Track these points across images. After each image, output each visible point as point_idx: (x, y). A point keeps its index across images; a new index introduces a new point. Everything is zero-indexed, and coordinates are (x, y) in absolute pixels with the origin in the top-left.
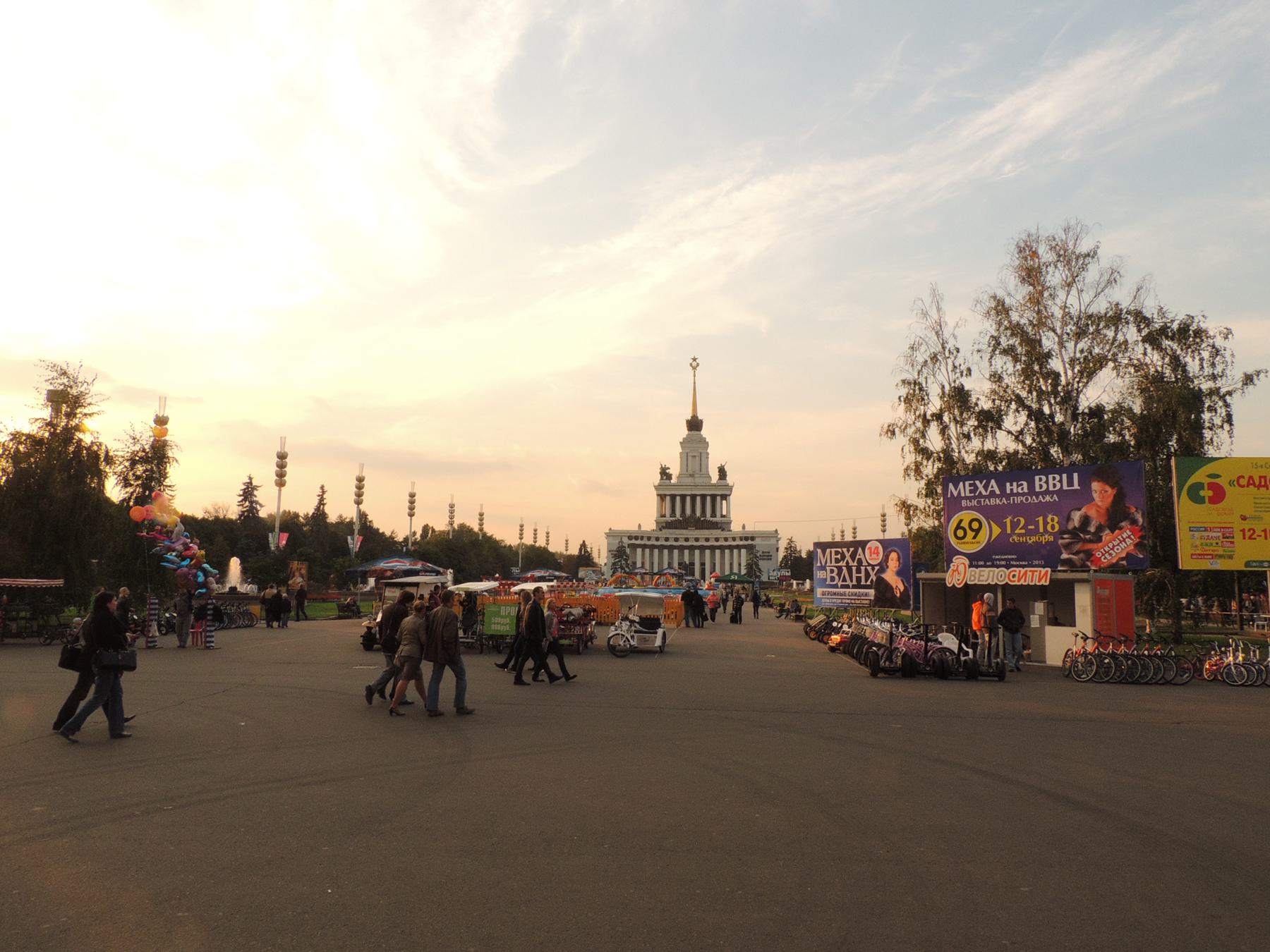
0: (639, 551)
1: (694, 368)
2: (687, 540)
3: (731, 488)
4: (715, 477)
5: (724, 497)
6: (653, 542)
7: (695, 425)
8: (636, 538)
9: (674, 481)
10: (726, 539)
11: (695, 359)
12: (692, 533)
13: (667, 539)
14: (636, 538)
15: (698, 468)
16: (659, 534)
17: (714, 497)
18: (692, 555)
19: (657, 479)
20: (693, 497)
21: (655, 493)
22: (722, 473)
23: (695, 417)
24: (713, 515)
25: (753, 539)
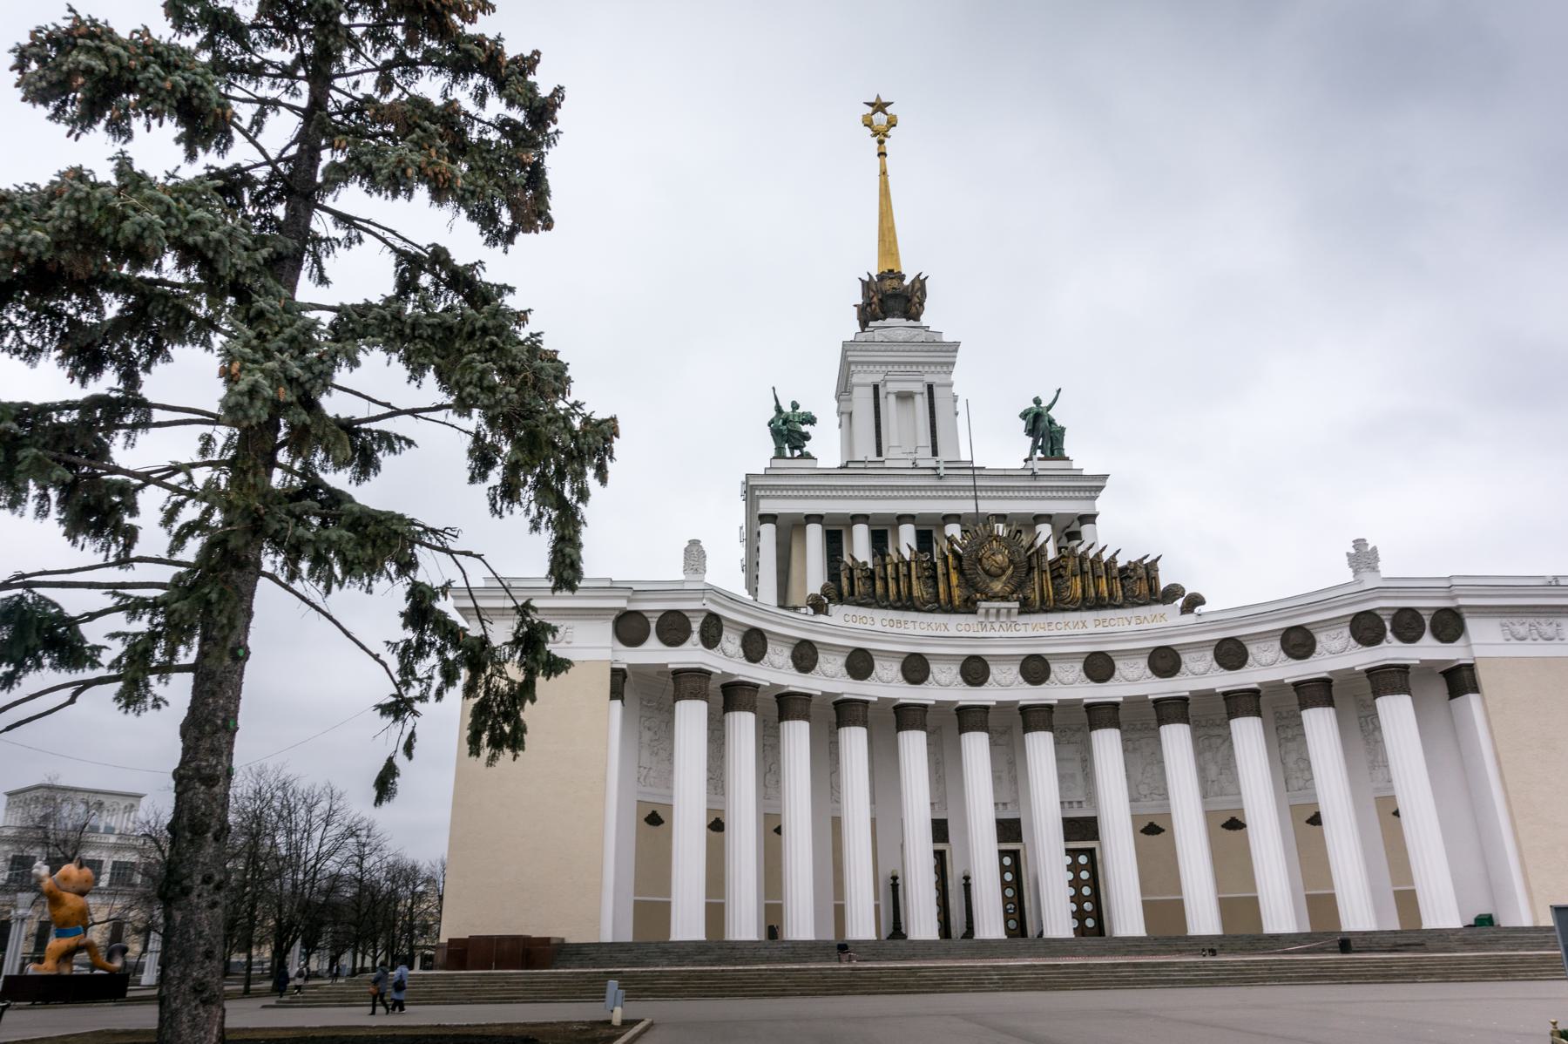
0: (691, 716)
1: (881, 135)
2: (975, 670)
3: (1094, 486)
6: (775, 672)
7: (891, 298)
8: (673, 628)
10: (1231, 653)
11: (879, 106)
12: (1003, 633)
13: (860, 664)
14: (673, 628)
15: (925, 439)
16: (801, 625)
18: (1010, 769)
19: (760, 453)
23: (894, 275)
25: (1449, 624)
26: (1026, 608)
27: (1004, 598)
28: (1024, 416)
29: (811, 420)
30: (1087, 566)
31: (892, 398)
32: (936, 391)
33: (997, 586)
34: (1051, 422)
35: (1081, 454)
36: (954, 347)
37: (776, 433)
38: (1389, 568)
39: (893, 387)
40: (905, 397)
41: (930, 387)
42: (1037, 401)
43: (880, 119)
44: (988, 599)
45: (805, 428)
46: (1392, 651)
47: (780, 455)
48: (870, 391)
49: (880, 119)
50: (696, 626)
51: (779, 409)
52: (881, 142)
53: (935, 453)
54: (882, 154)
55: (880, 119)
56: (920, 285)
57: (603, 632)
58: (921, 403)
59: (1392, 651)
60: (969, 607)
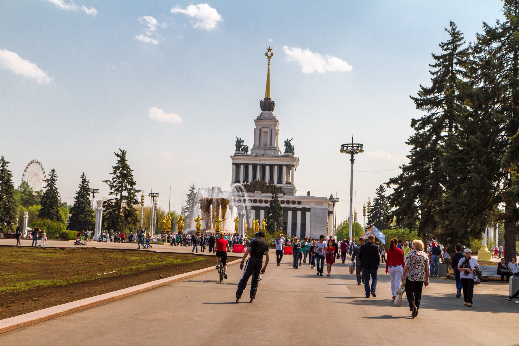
1: (269, 58)
5: (289, 167)
9: (249, 152)
11: (269, 50)
15: (269, 142)
17: (280, 167)
19: (233, 150)
20: (263, 166)
21: (231, 161)
22: (287, 144)
23: (267, 99)
24: (280, 181)
26: (262, 192)
29: (243, 141)
34: (290, 144)
41: (271, 130)
48: (259, 130)
49: (269, 54)
51: (238, 138)
53: (271, 145)
54: (269, 64)
55: (269, 54)
58: (269, 134)
60: (254, 192)
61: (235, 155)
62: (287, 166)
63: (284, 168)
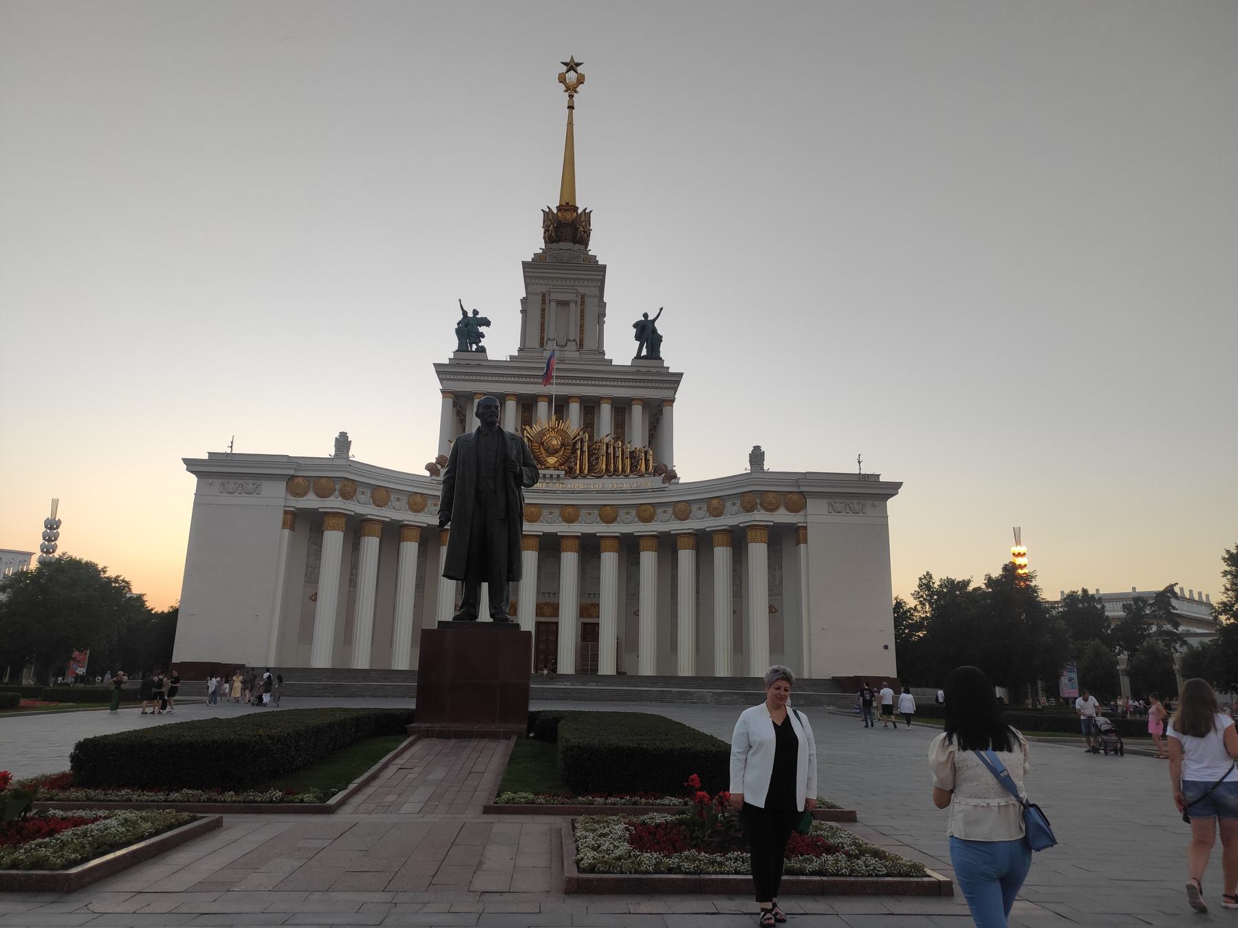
0: (333, 540)
1: (571, 90)
3: (674, 380)
4: (620, 347)
10: (682, 510)
11: (572, 66)
15: (574, 334)
19: (447, 347)
22: (647, 332)
23: (568, 206)
27: (556, 469)
28: (635, 326)
29: (487, 323)
30: (611, 450)
31: (553, 304)
32: (587, 300)
33: (552, 460)
34: (654, 330)
35: (671, 357)
36: (604, 267)
37: (458, 332)
38: (770, 465)
39: (553, 296)
40: (563, 304)
41: (583, 297)
42: (646, 315)
43: (572, 77)
44: (548, 468)
45: (482, 329)
46: (761, 516)
47: (462, 348)
48: (540, 297)
49: (572, 76)
50: (338, 487)
51: (465, 313)
52: (571, 96)
53: (581, 345)
54: (571, 107)
55: (572, 77)
56: (587, 215)
57: (282, 486)
58: (574, 310)
59: (761, 516)
61: (454, 363)
62: (645, 403)
63: (637, 410)
